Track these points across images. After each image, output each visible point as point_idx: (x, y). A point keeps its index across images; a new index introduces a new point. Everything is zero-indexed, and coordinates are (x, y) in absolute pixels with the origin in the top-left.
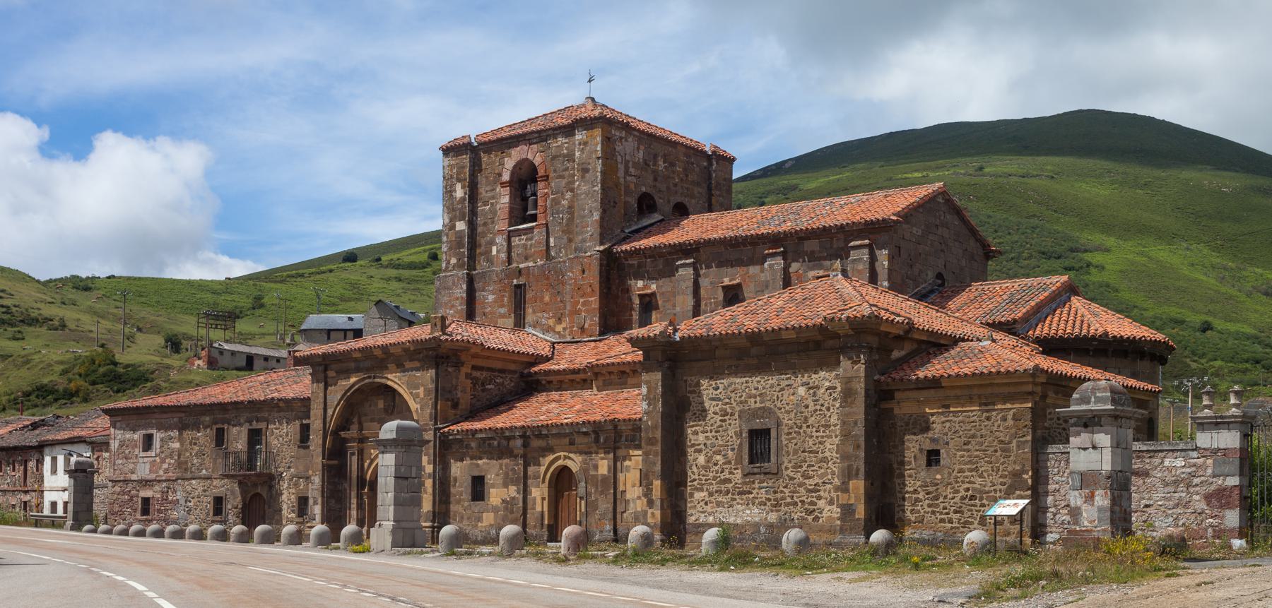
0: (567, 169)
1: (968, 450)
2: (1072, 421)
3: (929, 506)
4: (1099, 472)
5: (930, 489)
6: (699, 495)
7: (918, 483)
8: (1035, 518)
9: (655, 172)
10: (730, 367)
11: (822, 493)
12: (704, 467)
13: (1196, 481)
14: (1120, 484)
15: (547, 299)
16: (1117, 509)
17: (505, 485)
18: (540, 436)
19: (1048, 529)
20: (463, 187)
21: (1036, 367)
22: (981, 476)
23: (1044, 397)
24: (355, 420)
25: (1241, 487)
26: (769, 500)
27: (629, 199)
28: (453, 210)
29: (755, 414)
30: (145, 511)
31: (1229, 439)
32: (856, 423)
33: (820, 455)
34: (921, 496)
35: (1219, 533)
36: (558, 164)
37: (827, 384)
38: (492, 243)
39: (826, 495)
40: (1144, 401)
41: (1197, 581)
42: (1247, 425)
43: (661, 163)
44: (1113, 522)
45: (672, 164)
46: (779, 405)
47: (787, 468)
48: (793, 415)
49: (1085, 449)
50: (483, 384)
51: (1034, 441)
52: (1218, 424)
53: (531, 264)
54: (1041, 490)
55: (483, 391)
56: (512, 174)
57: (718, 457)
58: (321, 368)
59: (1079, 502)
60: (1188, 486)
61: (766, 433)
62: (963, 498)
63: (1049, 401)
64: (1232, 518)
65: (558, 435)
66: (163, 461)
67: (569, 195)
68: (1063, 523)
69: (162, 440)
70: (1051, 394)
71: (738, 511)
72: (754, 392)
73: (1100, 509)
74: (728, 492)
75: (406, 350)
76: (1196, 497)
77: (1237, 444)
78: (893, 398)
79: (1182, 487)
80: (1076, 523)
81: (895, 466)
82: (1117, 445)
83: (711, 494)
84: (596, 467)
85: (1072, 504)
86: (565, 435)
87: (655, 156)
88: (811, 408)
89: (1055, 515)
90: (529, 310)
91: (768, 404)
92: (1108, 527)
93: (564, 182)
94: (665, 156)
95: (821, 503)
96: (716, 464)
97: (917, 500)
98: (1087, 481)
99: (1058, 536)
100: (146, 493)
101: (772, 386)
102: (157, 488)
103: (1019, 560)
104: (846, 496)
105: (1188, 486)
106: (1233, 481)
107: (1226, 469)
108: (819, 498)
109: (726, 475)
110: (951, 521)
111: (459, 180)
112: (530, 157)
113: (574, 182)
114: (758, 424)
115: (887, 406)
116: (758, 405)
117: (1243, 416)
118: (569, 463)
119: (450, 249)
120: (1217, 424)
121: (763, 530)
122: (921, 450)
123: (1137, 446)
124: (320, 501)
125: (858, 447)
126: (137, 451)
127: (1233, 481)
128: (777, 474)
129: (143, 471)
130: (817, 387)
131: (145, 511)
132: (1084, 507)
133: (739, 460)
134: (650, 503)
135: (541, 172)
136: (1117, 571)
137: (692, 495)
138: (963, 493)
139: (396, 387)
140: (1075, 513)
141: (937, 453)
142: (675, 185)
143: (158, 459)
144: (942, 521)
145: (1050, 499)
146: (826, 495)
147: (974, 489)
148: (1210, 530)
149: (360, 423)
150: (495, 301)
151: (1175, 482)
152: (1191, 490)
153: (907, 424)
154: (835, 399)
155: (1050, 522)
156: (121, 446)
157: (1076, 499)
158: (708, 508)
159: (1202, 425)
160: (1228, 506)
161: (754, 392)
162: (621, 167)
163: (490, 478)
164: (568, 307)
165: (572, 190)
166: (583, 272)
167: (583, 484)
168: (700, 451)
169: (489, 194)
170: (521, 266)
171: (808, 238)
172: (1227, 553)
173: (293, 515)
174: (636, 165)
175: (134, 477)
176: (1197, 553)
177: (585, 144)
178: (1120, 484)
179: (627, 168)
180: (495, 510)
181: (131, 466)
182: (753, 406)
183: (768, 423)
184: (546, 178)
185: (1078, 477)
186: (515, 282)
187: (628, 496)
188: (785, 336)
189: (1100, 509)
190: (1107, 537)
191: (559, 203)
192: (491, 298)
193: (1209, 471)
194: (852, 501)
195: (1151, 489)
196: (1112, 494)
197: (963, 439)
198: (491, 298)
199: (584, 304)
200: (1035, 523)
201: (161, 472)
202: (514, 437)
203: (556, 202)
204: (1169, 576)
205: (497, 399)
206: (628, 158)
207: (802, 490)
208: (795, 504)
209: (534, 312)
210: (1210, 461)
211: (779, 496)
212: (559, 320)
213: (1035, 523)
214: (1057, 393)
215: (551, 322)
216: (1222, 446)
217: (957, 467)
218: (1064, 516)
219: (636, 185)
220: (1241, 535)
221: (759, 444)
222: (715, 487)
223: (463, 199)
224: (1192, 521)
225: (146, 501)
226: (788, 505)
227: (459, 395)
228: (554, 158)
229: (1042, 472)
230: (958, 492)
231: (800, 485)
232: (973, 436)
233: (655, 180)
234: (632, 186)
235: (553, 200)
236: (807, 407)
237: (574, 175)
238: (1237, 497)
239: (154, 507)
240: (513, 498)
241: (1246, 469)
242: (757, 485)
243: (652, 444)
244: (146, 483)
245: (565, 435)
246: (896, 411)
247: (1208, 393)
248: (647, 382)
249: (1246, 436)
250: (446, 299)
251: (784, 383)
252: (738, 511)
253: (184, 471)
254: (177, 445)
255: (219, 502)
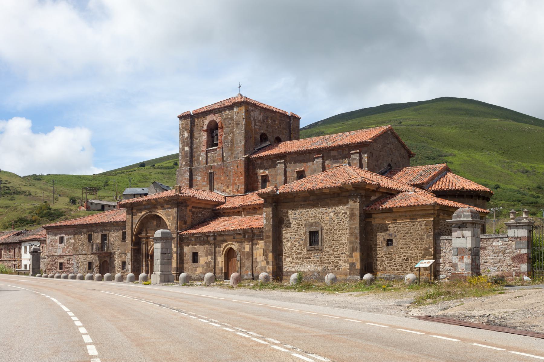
0: (230, 124)
1: (405, 239)
2: (453, 226)
3: (388, 263)
4: (466, 248)
5: (388, 256)
6: (288, 260)
7: (383, 254)
8: (435, 268)
9: (267, 124)
10: (301, 205)
11: (341, 258)
12: (290, 248)
13: (508, 251)
14: (475, 253)
15: (223, 178)
16: (474, 264)
17: (207, 256)
18: (221, 235)
19: (441, 273)
20: (187, 133)
21: (435, 203)
22: (411, 250)
23: (438, 215)
24: (144, 230)
25: (528, 254)
26: (318, 261)
27: (256, 136)
28: (184, 142)
29: (312, 225)
30: (61, 268)
31: (523, 233)
32: (356, 228)
33: (340, 242)
34: (384, 259)
35: (518, 274)
36: (227, 122)
37: (343, 211)
38: (200, 155)
39: (343, 259)
40: (482, 216)
41: (515, 296)
42: (531, 227)
43: (269, 120)
44: (472, 269)
45: (274, 121)
46: (322, 220)
47: (326, 248)
48: (328, 225)
49: (459, 238)
50: (197, 214)
51: (434, 234)
52: (517, 226)
53: (216, 164)
54: (437, 256)
55: (197, 217)
56: (208, 126)
57: (296, 243)
58: (130, 209)
59: (457, 261)
60: (504, 253)
61: (316, 233)
62: (403, 260)
63: (440, 217)
64: (524, 267)
65: (228, 235)
66: (67, 248)
67: (231, 135)
68: (447, 270)
69: (67, 239)
70: (441, 214)
71: (305, 266)
72: (311, 215)
73: (466, 264)
74: (300, 258)
75: (165, 200)
76: (507, 258)
77: (526, 235)
78: (372, 217)
79: (501, 254)
80: (455, 270)
81: (373, 246)
82: (473, 236)
83: (293, 259)
84: (244, 248)
85: (454, 262)
86: (231, 235)
87: (267, 118)
88: (336, 222)
89: (444, 267)
90: (215, 183)
91: (317, 220)
92: (470, 272)
93: (229, 129)
94: (271, 117)
95: (341, 262)
96: (295, 246)
97: (383, 261)
98: (460, 251)
99: (445, 276)
100: (61, 261)
101: (319, 213)
102: (65, 259)
103: (430, 286)
104: (352, 259)
105: (504, 253)
106: (525, 251)
107: (521, 246)
108: (340, 260)
109: (300, 251)
110: (397, 270)
112: (215, 119)
113: (233, 129)
114: (313, 229)
115: (369, 220)
116: (313, 221)
117: (529, 222)
118: (233, 247)
119: (182, 158)
120: (517, 226)
121: (316, 274)
122: (384, 239)
123: (482, 236)
124: (130, 263)
125: (357, 238)
126: (57, 244)
127: (525, 251)
128: (321, 250)
129: (60, 252)
130: (339, 213)
131: (61, 268)
132: (459, 263)
133: (305, 244)
134: (268, 263)
135: (220, 125)
136: (476, 292)
137: (285, 259)
138: (403, 257)
139: (161, 216)
140: (455, 266)
141: (391, 240)
142: (276, 129)
143: (65, 247)
144: (394, 269)
145: (441, 260)
146: (343, 259)
147: (408, 256)
148: (514, 273)
149: (146, 231)
150: (201, 180)
151: (498, 252)
152: (505, 255)
153: (378, 228)
154: (346, 218)
155: (441, 270)
156: (51, 242)
157: (455, 260)
158: (292, 265)
159: (510, 227)
160: (522, 262)
161: (311, 215)
162: (253, 122)
163: (200, 253)
164: (232, 181)
165: (233, 133)
166: (238, 166)
167: (239, 255)
168: (288, 241)
169: (198, 135)
170: (212, 165)
171: (333, 150)
172: (523, 283)
173: (120, 269)
174: (259, 121)
175: (56, 254)
176: (509, 283)
177: (238, 113)
178: (475, 253)
179: (255, 123)
180: (202, 266)
181: (55, 250)
182: (311, 221)
183: (318, 228)
184: (222, 128)
185: (456, 250)
186: (209, 171)
187: (258, 260)
188: (324, 191)
189: (466, 264)
190: (470, 276)
192: (199, 178)
193: (514, 247)
194: (354, 262)
195: (486, 255)
196: (472, 257)
197: (403, 234)
198: (199, 178)
199: (238, 180)
200: (435, 271)
201: (67, 252)
202: (210, 236)
203: (226, 138)
204: (500, 293)
205: (202, 220)
206: (256, 118)
207: (332, 257)
208: (330, 263)
209: (217, 184)
210: (514, 243)
211: (322, 259)
212: (228, 187)
213: (435, 271)
214: (444, 214)
215: (224, 188)
216: (519, 236)
217: (400, 246)
218: (448, 267)
219: (259, 130)
220: (528, 275)
221: (314, 237)
222: (295, 256)
223: (188, 137)
224: (506, 269)
225: (61, 264)
226: (326, 263)
227: (187, 218)
228: (225, 119)
229: (438, 248)
230: (400, 257)
231: (332, 255)
232: (407, 233)
233: (267, 127)
234: (258, 130)
236: (334, 221)
237: (233, 126)
238: (526, 258)
239: (64, 266)
240: (210, 261)
241: (530, 246)
242: (313, 255)
243: (268, 238)
244: (61, 257)
245: (231, 235)
246: (373, 223)
247: (513, 213)
248: (266, 212)
249: (530, 231)
250: (181, 179)
251: (324, 211)
252: (305, 266)
253: (76, 252)
254: (73, 241)
255: (90, 264)
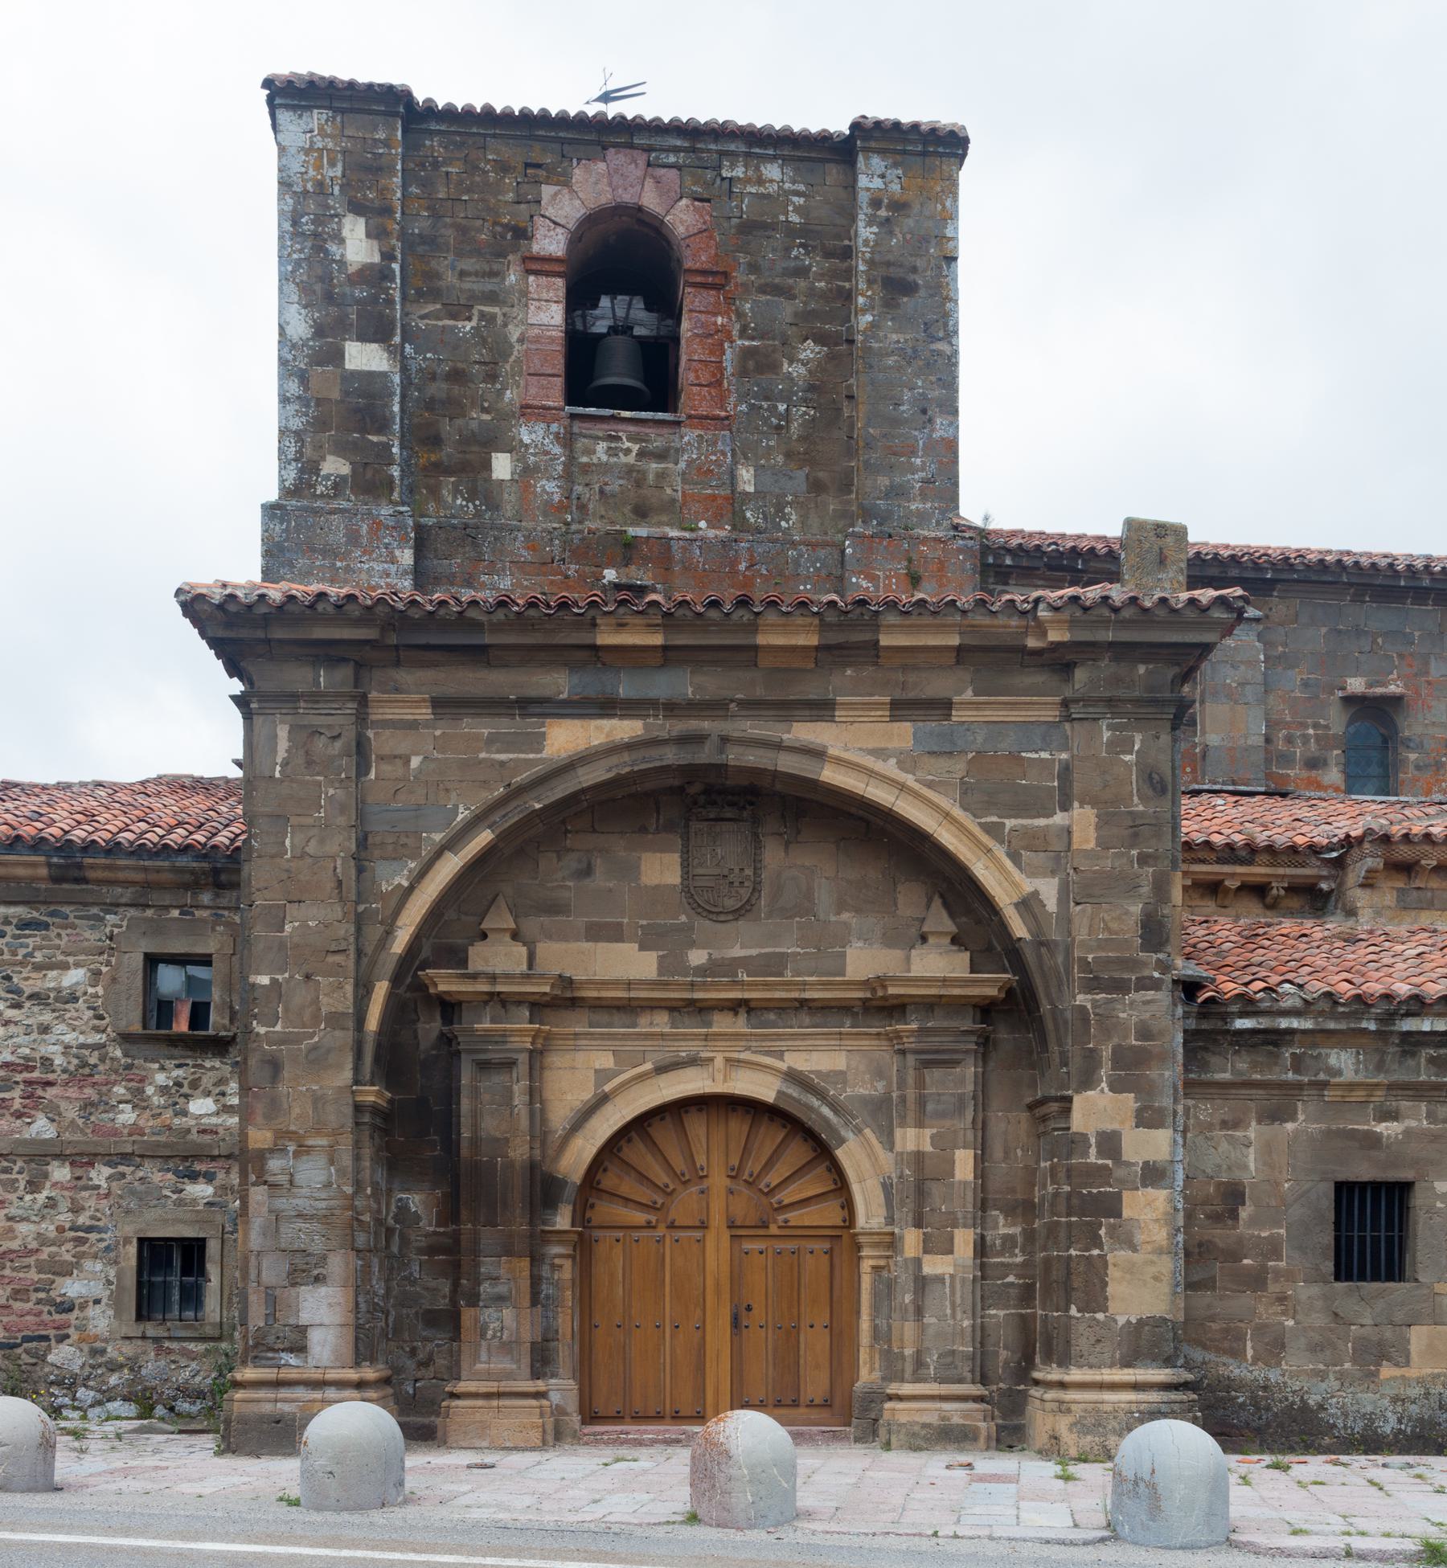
0: (802, 272)
56: (576, 239)
67: (809, 351)
111: (357, 208)
112: (650, 200)
169: (469, 284)
170: (633, 531)
191: (775, 367)
203: (758, 364)
228: (750, 228)
235: (747, 354)
